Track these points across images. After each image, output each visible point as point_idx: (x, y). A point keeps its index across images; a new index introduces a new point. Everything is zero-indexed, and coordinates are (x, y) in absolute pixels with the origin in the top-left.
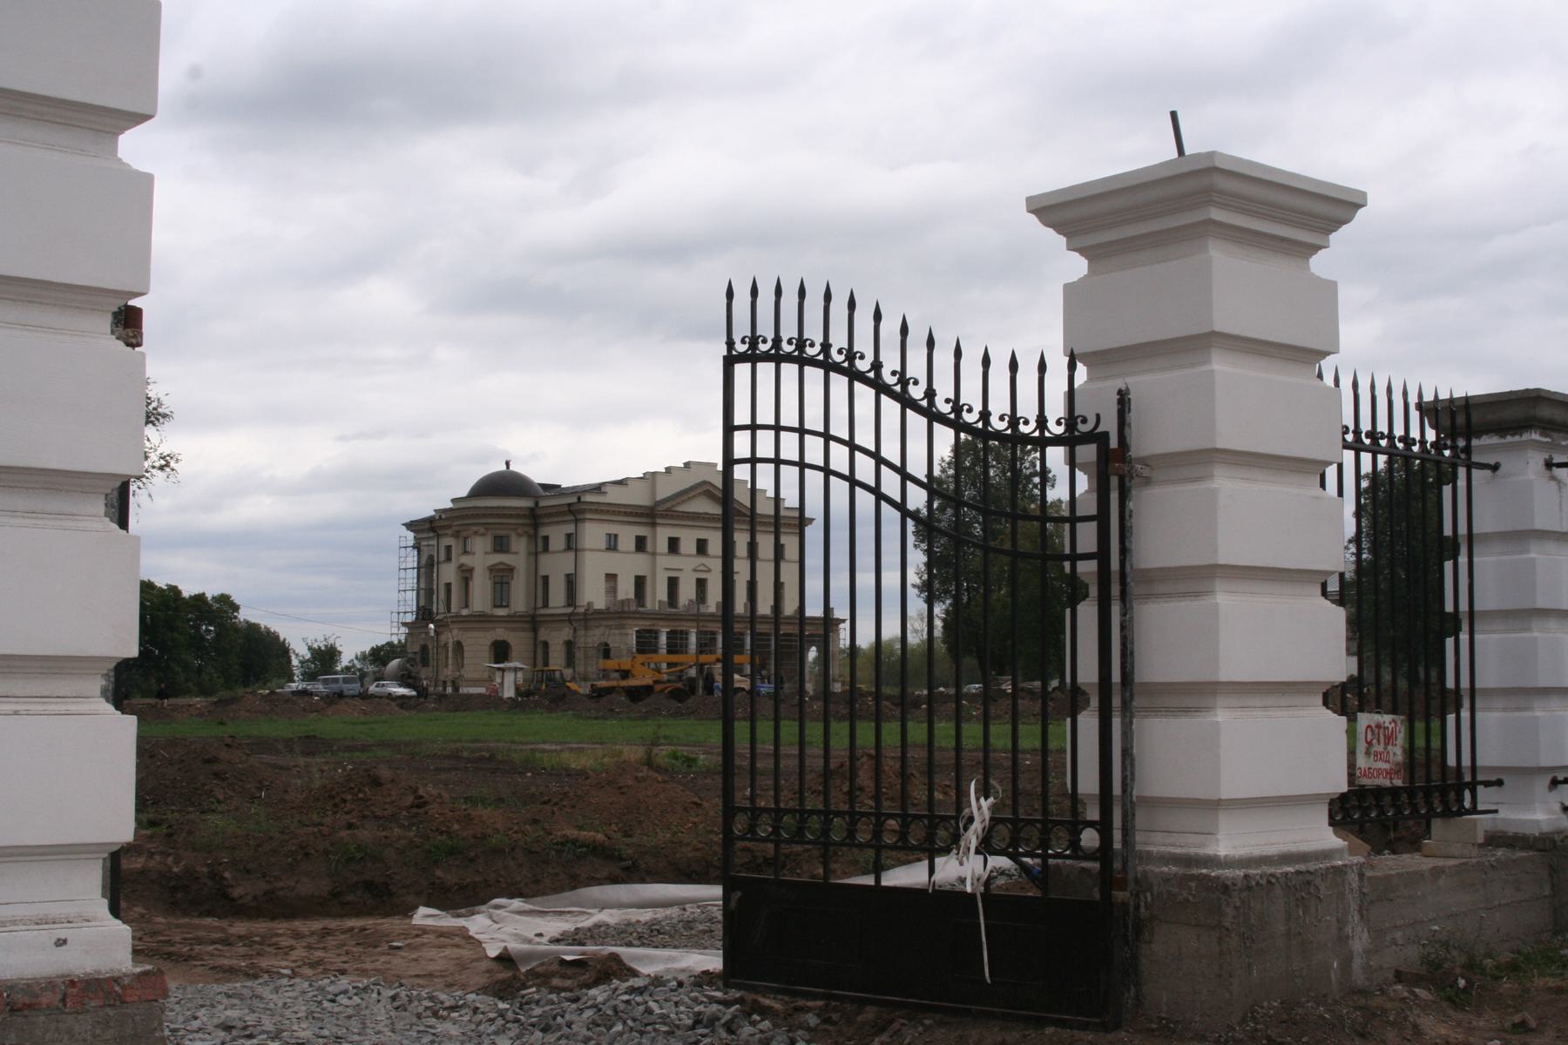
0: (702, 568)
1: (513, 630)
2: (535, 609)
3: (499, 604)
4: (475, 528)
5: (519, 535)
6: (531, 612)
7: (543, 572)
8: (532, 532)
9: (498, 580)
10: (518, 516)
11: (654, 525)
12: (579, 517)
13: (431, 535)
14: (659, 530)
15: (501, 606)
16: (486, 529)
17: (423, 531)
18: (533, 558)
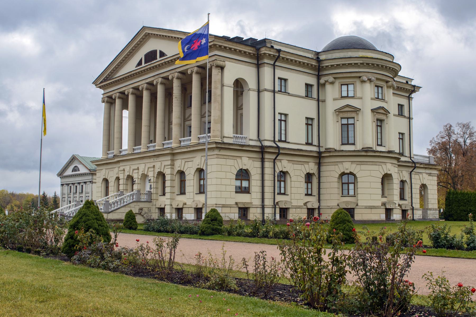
3: (346, 142)
5: (363, 82)
9: (345, 121)
15: (348, 144)
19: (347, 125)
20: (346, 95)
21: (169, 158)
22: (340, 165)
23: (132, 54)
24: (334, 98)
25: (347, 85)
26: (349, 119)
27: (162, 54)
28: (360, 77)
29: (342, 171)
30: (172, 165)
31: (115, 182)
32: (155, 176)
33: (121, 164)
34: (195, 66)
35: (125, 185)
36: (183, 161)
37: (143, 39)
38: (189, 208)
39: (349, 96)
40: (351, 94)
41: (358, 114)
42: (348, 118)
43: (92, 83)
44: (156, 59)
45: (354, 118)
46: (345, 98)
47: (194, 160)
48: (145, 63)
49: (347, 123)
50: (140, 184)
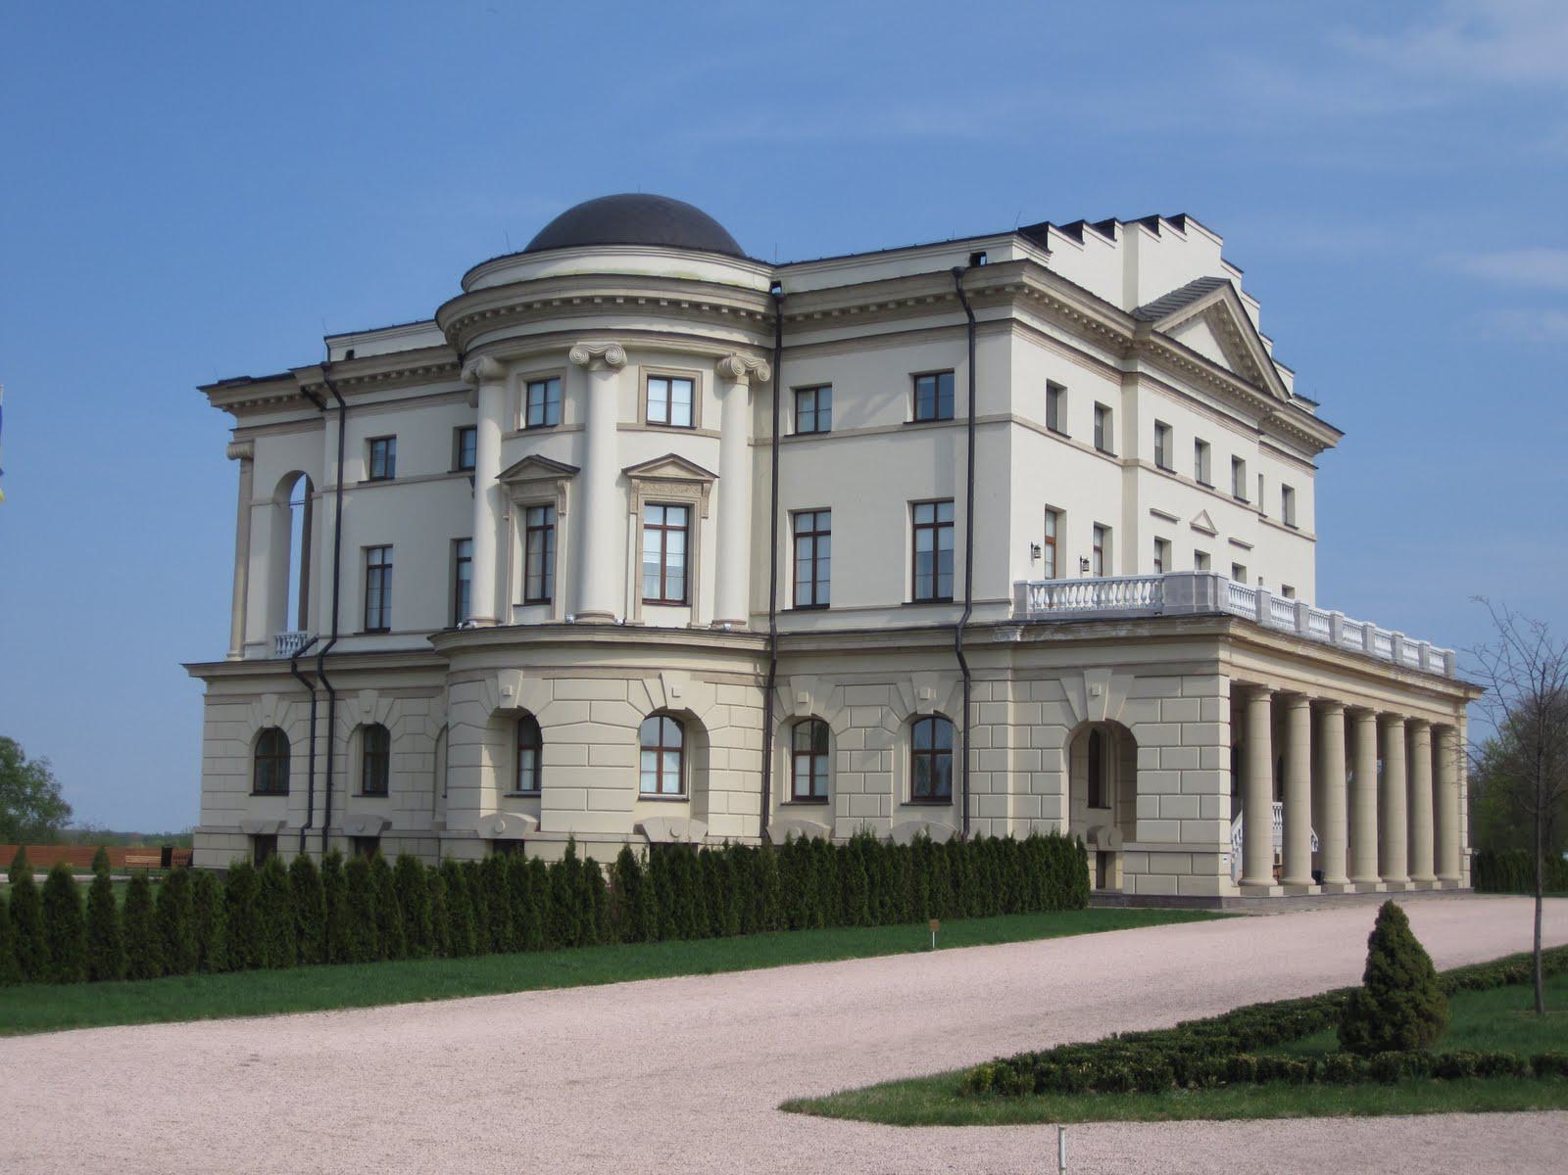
0: (1203, 523)
1: (715, 678)
2: (772, 615)
3: (657, 596)
4: (597, 345)
6: (764, 627)
7: (790, 500)
8: (765, 372)
10: (733, 317)
11: (1127, 378)
12: (981, 315)
13: (312, 412)
14: (1144, 393)
15: (662, 602)
16: (628, 350)
17: (267, 405)
18: (767, 455)
19: (658, 534)
20: (663, 419)
22: (653, 684)
24: (618, 424)
25: (669, 380)
26: (668, 509)
28: (718, 358)
29: (659, 704)
39: (672, 424)
40: (680, 417)
41: (705, 493)
42: (665, 506)
45: (688, 508)
46: (657, 429)
49: (660, 523)
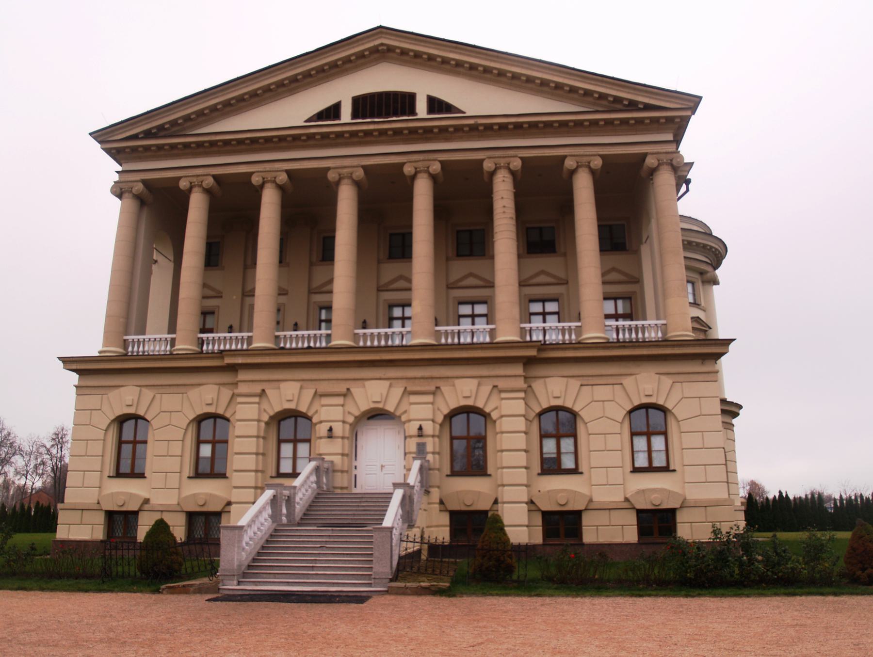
21: (518, 370)
23: (293, 85)
27: (436, 105)
30: (528, 391)
31: (186, 430)
32: (440, 418)
33: (242, 375)
34: (595, 153)
35: (261, 440)
36: (575, 384)
37: (361, 56)
38: (612, 512)
43: (91, 134)
44: (412, 111)
47: (628, 382)
48: (355, 115)
50: (348, 438)
